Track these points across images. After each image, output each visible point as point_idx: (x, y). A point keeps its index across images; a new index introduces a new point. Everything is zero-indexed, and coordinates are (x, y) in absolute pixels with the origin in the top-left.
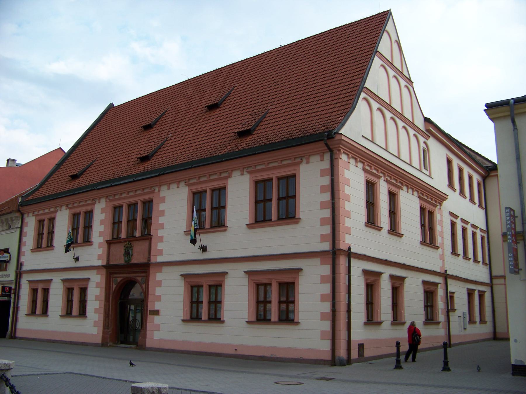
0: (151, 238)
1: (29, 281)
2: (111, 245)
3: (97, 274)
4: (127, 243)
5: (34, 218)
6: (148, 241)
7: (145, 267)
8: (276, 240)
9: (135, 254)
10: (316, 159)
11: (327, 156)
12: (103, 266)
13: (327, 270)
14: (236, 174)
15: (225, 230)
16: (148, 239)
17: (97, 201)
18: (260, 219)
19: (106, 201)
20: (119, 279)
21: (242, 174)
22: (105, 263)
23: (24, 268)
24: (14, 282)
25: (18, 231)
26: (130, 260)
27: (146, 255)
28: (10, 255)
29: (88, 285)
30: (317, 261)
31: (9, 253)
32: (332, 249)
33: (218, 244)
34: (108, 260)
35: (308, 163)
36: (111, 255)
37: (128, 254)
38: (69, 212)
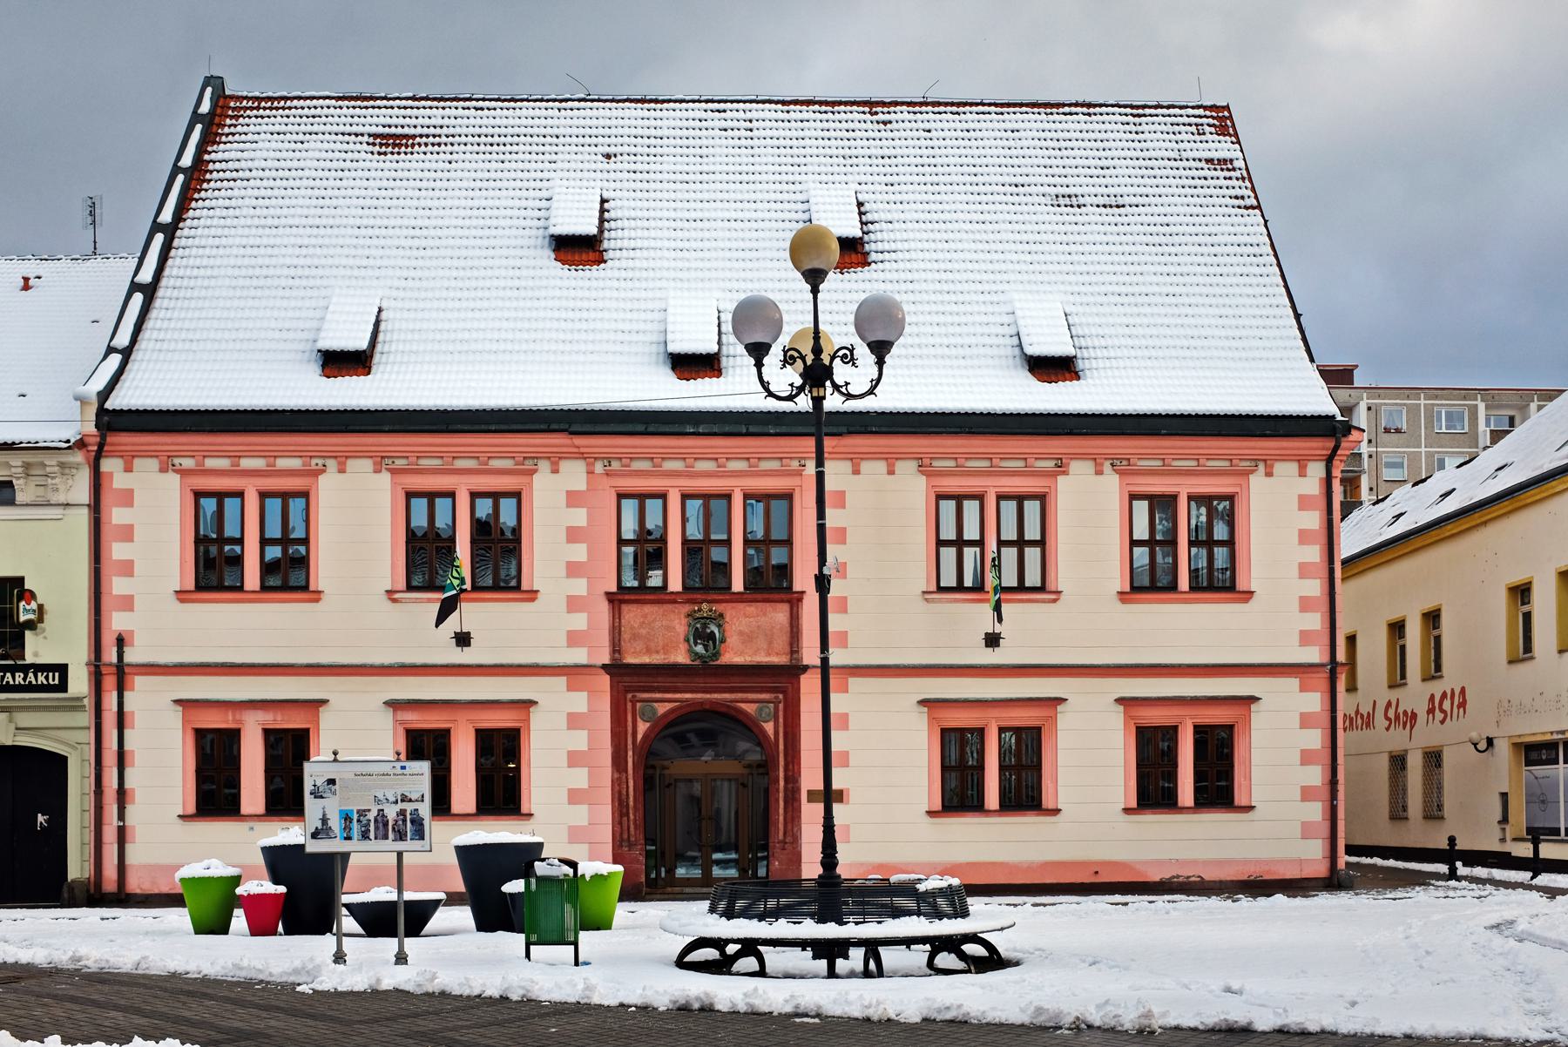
0: (800, 600)
1: (178, 702)
2: (625, 608)
3: (570, 688)
4: (704, 606)
5: (173, 480)
6: (786, 607)
7: (784, 677)
8: (1187, 629)
9: (733, 640)
10: (1286, 470)
11: (1317, 470)
12: (604, 667)
13: (1314, 702)
14: (1080, 471)
15: (1055, 601)
16: (789, 601)
17: (544, 466)
18: (1150, 584)
19: (590, 472)
20: (662, 709)
21: (1099, 472)
22: (607, 660)
23: (131, 656)
24: (88, 703)
25: (82, 517)
26: (716, 655)
27: (782, 642)
28: (41, 607)
29: (528, 720)
30: (1293, 683)
31: (32, 595)
32: (1326, 659)
33: (1030, 631)
34: (616, 648)
35: (1269, 474)
36: (626, 636)
37: (701, 635)
38: (394, 484)
